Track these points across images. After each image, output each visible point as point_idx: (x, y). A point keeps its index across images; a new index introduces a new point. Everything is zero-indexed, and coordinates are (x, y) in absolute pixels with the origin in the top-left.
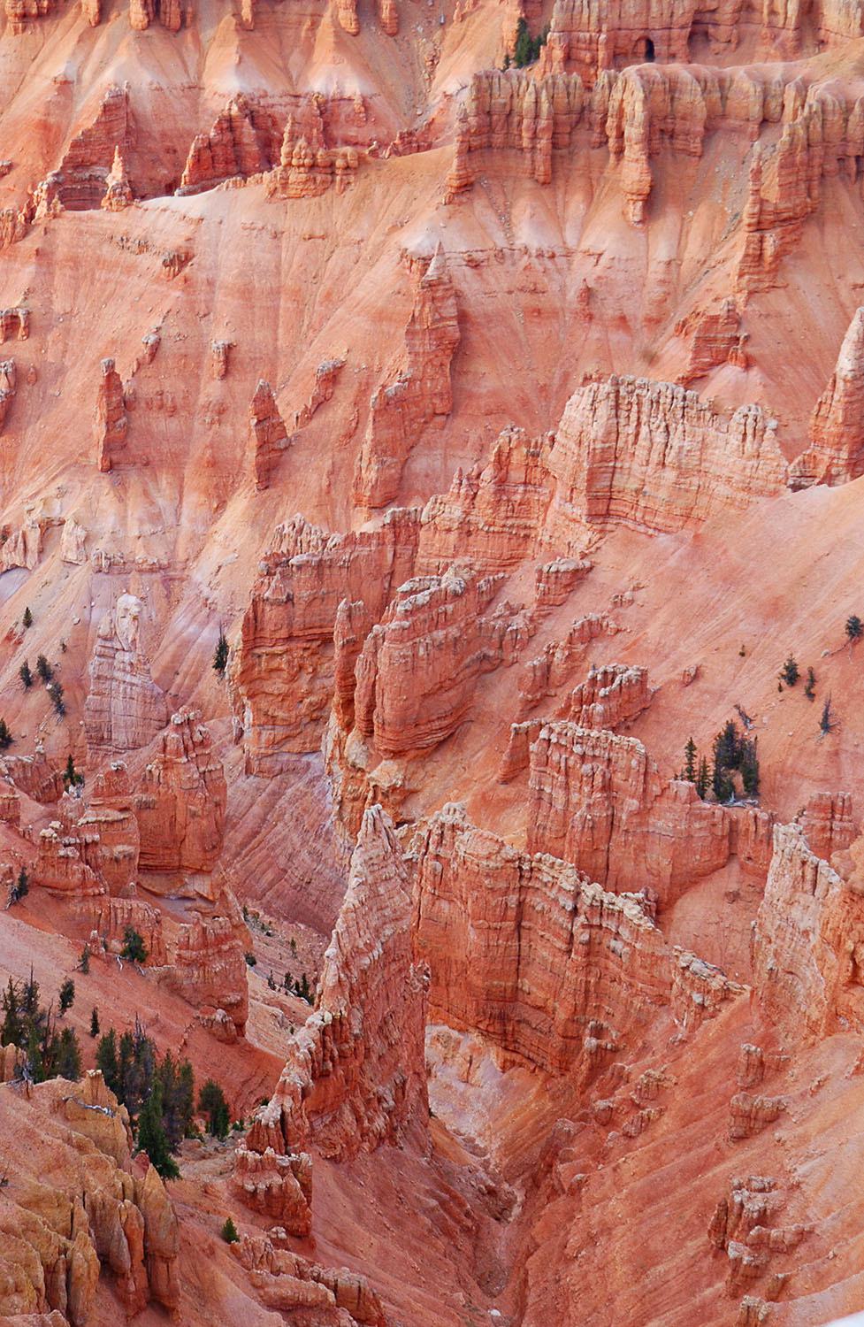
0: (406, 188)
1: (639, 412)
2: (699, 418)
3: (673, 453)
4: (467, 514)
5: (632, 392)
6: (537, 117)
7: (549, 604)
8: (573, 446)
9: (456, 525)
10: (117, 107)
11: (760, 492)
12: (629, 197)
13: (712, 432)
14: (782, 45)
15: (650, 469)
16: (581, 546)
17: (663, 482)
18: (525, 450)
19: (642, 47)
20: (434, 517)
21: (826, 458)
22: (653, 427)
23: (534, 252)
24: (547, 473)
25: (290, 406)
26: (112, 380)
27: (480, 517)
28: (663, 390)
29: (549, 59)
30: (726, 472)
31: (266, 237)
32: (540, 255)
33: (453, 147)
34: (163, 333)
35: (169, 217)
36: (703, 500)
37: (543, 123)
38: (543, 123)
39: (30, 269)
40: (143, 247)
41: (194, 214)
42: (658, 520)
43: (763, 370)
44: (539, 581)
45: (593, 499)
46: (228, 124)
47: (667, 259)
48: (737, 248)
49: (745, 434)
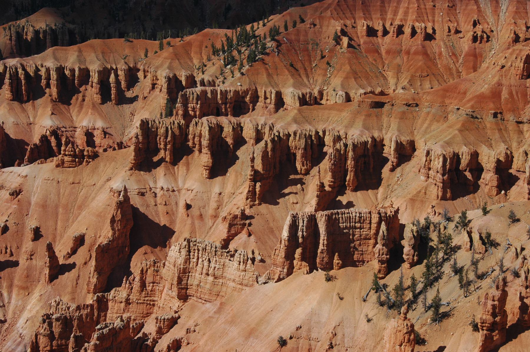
0: (113, 163)
1: (198, 253)
2: (222, 256)
3: (212, 269)
4: (129, 295)
5: (195, 245)
6: (166, 137)
7: (160, 332)
8: (172, 266)
9: (124, 300)
11: (246, 286)
12: (204, 167)
13: (227, 261)
14: (270, 110)
15: (203, 276)
16: (175, 308)
17: (208, 281)
18: (153, 269)
19: (215, 111)
20: (115, 297)
21: (278, 271)
22: (204, 259)
23: (165, 189)
24: (162, 278)
25: (61, 250)
27: (133, 297)
28: (208, 244)
29: (177, 114)
30: (233, 277)
31: (55, 184)
32: (168, 190)
33: (132, 147)
34: (8, 223)
36: (224, 289)
37: (169, 139)
38: (169, 139)
41: (24, 174)
42: (206, 297)
43: (255, 236)
44: (157, 323)
45: (180, 289)
46: (44, 139)
47: (219, 192)
48: (245, 189)
49: (240, 262)
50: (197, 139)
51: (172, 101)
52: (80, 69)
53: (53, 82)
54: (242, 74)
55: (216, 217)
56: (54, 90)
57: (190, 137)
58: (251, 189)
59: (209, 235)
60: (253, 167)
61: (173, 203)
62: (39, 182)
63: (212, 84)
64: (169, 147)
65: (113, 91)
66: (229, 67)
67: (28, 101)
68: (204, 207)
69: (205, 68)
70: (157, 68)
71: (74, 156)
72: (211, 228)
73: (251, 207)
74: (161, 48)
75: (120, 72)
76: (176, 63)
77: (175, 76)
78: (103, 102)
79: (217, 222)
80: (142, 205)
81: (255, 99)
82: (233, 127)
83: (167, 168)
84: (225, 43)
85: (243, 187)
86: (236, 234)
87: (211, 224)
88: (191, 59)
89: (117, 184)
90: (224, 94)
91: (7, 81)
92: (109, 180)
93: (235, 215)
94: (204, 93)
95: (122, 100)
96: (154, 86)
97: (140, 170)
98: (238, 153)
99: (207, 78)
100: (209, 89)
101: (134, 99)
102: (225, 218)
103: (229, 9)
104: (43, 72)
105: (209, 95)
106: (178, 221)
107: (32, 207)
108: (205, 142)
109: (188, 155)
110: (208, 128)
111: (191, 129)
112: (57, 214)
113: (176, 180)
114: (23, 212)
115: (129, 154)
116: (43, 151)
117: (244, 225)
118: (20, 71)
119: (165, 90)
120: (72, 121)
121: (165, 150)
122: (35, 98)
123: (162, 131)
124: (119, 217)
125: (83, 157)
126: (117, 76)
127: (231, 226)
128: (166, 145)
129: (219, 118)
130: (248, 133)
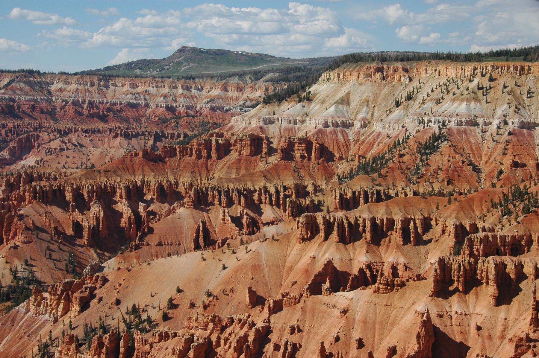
6: (459, 272)
10: (329, 264)
19: (495, 251)
23: (459, 313)
26: (323, 349)
29: (464, 253)
31: (373, 305)
33: (432, 279)
35: (343, 297)
37: (461, 273)
38: (461, 273)
39: (300, 313)
40: (334, 307)
41: (350, 297)
46: (361, 271)
48: (528, 316)
50: (484, 274)
51: (459, 243)
52: (387, 219)
53: (368, 229)
54: (518, 223)
55: (503, 338)
56: (368, 235)
57: (479, 272)
58: (534, 317)
59: (497, 353)
60: (535, 298)
61: (466, 325)
62: (361, 303)
63: (492, 230)
64: (461, 279)
65: (412, 235)
66: (506, 217)
67: (349, 243)
68: (492, 329)
69: (485, 218)
70: (447, 217)
71: (387, 284)
72: (499, 347)
73: (535, 331)
74: (449, 202)
75: (417, 221)
76: (462, 214)
77: (461, 224)
78: (405, 243)
79: (504, 342)
80: (441, 325)
81: (530, 242)
82: (515, 265)
83: (460, 297)
84: (502, 199)
85: (526, 314)
86: (523, 354)
87: (498, 344)
88: (473, 211)
89: (420, 307)
90: (503, 238)
91: (335, 229)
92: (413, 304)
93: (521, 338)
94: (487, 237)
95: (419, 242)
96: (443, 232)
97: (438, 297)
98: (521, 285)
99: (487, 225)
100: (490, 234)
101: (430, 241)
102: (511, 339)
103: (501, 172)
104: (360, 221)
105: (491, 239)
106: (470, 339)
107: (356, 323)
108: (491, 277)
109: (477, 287)
110: (494, 265)
111: (479, 265)
112: (375, 329)
113: (467, 306)
114: (349, 326)
115: (429, 284)
116: (362, 280)
117: (530, 346)
118: (345, 221)
119: (452, 234)
120: (381, 258)
121: (458, 281)
122: (355, 240)
123: (455, 267)
124: (423, 334)
125: (393, 286)
126: (415, 224)
127: (517, 347)
128: (458, 278)
129: (503, 258)
130: (528, 269)
